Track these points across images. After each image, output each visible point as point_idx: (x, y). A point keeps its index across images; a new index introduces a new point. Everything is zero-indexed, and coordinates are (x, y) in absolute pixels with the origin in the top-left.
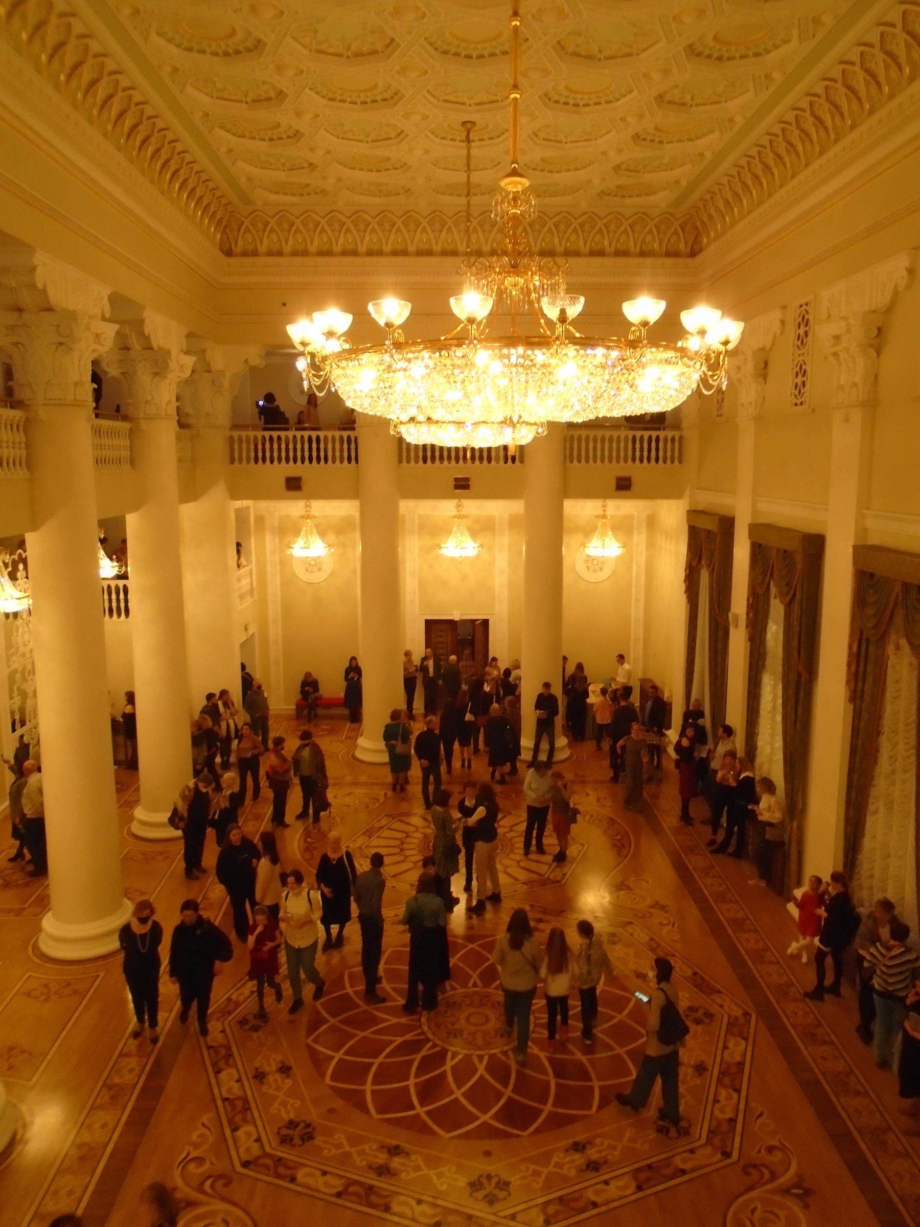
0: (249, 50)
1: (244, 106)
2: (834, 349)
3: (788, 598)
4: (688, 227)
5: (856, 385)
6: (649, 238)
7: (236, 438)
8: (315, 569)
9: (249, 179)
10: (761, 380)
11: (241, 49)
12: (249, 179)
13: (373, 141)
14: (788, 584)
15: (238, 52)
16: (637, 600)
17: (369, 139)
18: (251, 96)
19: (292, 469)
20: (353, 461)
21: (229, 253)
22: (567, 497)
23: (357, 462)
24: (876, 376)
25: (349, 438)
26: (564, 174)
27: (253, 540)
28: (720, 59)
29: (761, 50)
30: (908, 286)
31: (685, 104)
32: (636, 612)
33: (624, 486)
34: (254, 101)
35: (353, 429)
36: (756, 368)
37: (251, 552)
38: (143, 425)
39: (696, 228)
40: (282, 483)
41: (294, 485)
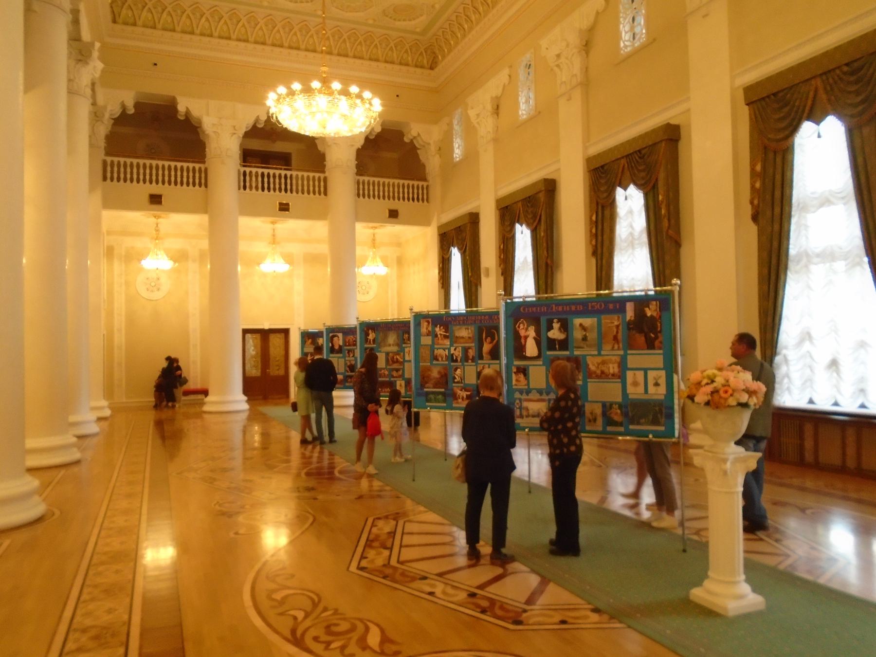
3: (535, 224)
4: (429, 52)
5: (576, 75)
7: (109, 163)
14: (535, 217)
19: (155, 189)
23: (206, 186)
24: (587, 68)
30: (604, 10)
33: (393, 214)
35: (204, 162)
39: (434, 53)
40: (146, 198)
41: (156, 199)
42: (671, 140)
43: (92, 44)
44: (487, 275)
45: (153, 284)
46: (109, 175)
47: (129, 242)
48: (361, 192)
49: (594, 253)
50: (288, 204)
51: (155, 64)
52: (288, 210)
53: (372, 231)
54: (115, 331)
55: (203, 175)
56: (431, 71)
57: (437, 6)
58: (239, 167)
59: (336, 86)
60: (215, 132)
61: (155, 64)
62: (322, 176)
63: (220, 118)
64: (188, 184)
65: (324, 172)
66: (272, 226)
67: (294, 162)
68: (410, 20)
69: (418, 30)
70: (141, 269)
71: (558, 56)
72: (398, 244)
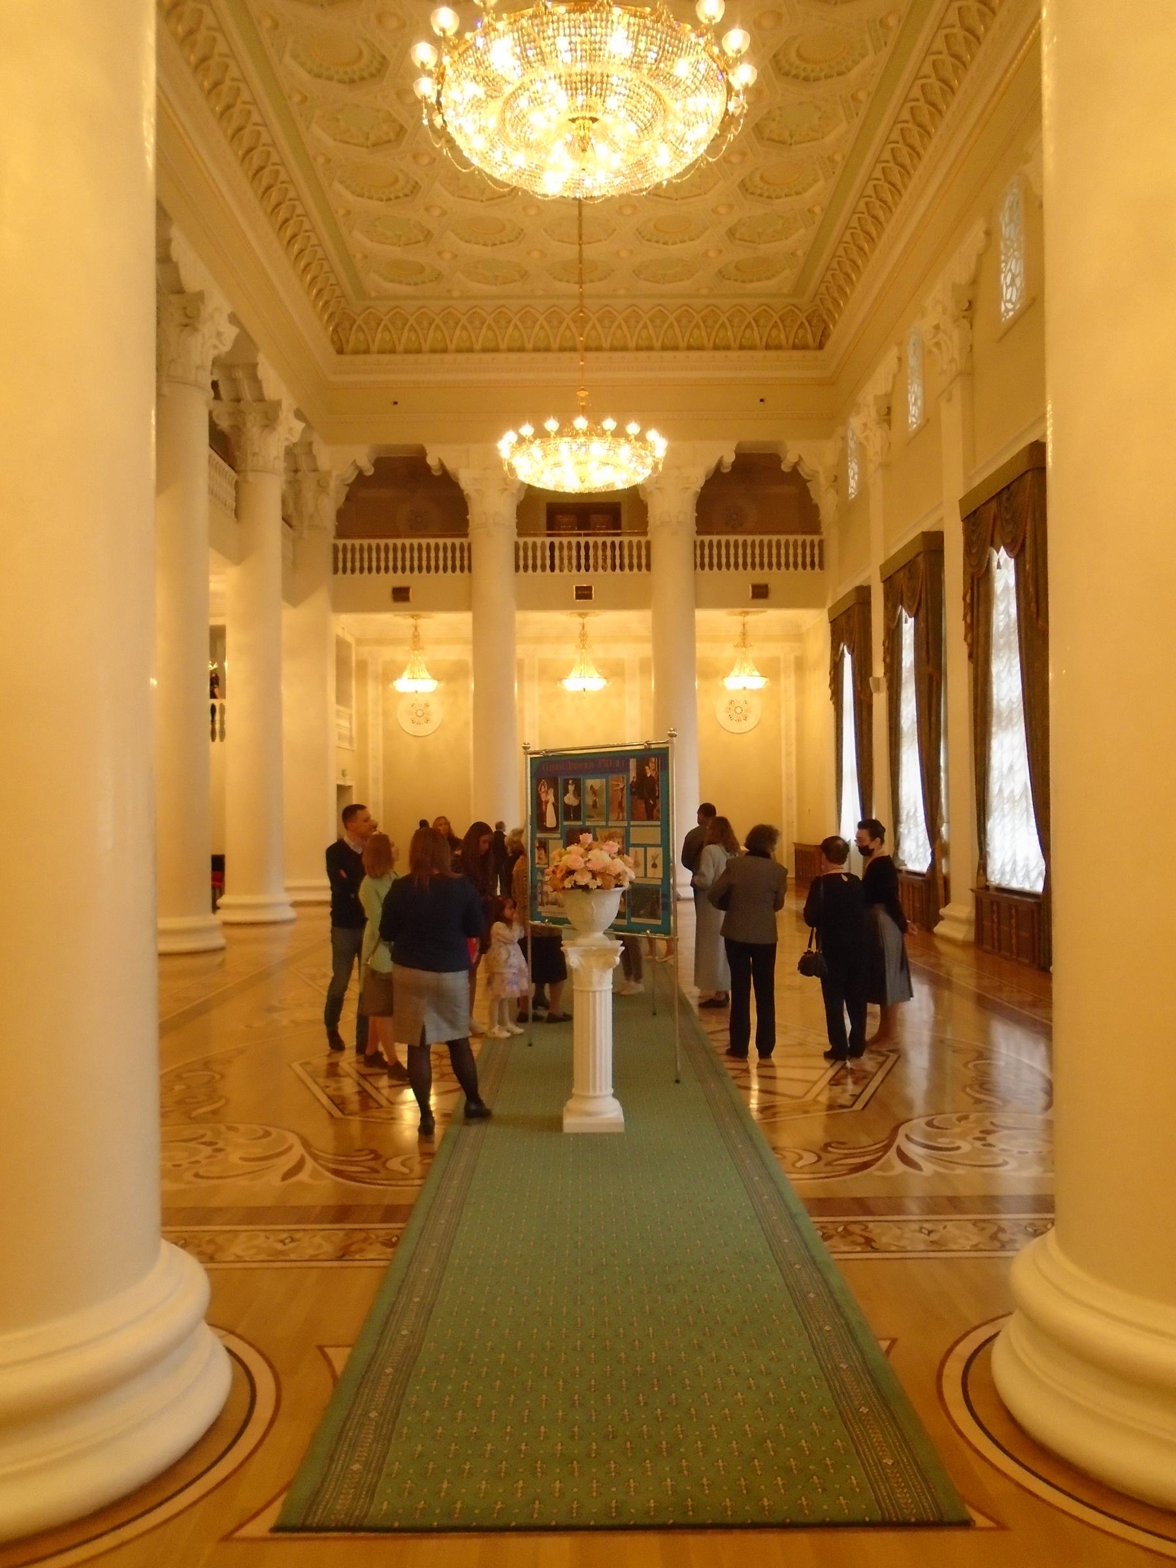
0: (372, 75)
1: (364, 150)
2: (936, 340)
4: (814, 322)
6: (774, 333)
7: (341, 547)
8: (423, 720)
9: (366, 257)
10: (886, 425)
11: (365, 74)
12: (366, 257)
13: (488, 200)
15: (362, 79)
16: (788, 754)
17: (484, 198)
18: (372, 138)
20: (466, 570)
21: (340, 352)
22: (698, 605)
25: (462, 546)
26: (679, 246)
27: (354, 682)
28: (806, 79)
29: (843, 68)
31: (783, 143)
32: (788, 767)
33: (760, 593)
34: (374, 145)
35: (466, 535)
36: (878, 412)
37: (350, 696)
38: (250, 477)
39: (824, 321)
41: (401, 595)
42: (1038, 469)
43: (278, 403)
44: (878, 690)
45: (420, 713)
46: (340, 565)
47: (388, 653)
48: (703, 560)
49: (970, 656)
50: (589, 588)
51: (396, 403)
52: (589, 597)
53: (740, 618)
54: (371, 781)
55: (466, 555)
56: (819, 353)
57: (800, 253)
58: (516, 538)
59: (581, 423)
60: (477, 491)
61: (396, 403)
62: (643, 540)
63: (485, 469)
64: (454, 570)
65: (645, 533)
66: (580, 620)
67: (625, 520)
68: (768, 278)
69: (785, 291)
70: (401, 695)
71: (937, 327)
72: (797, 636)
